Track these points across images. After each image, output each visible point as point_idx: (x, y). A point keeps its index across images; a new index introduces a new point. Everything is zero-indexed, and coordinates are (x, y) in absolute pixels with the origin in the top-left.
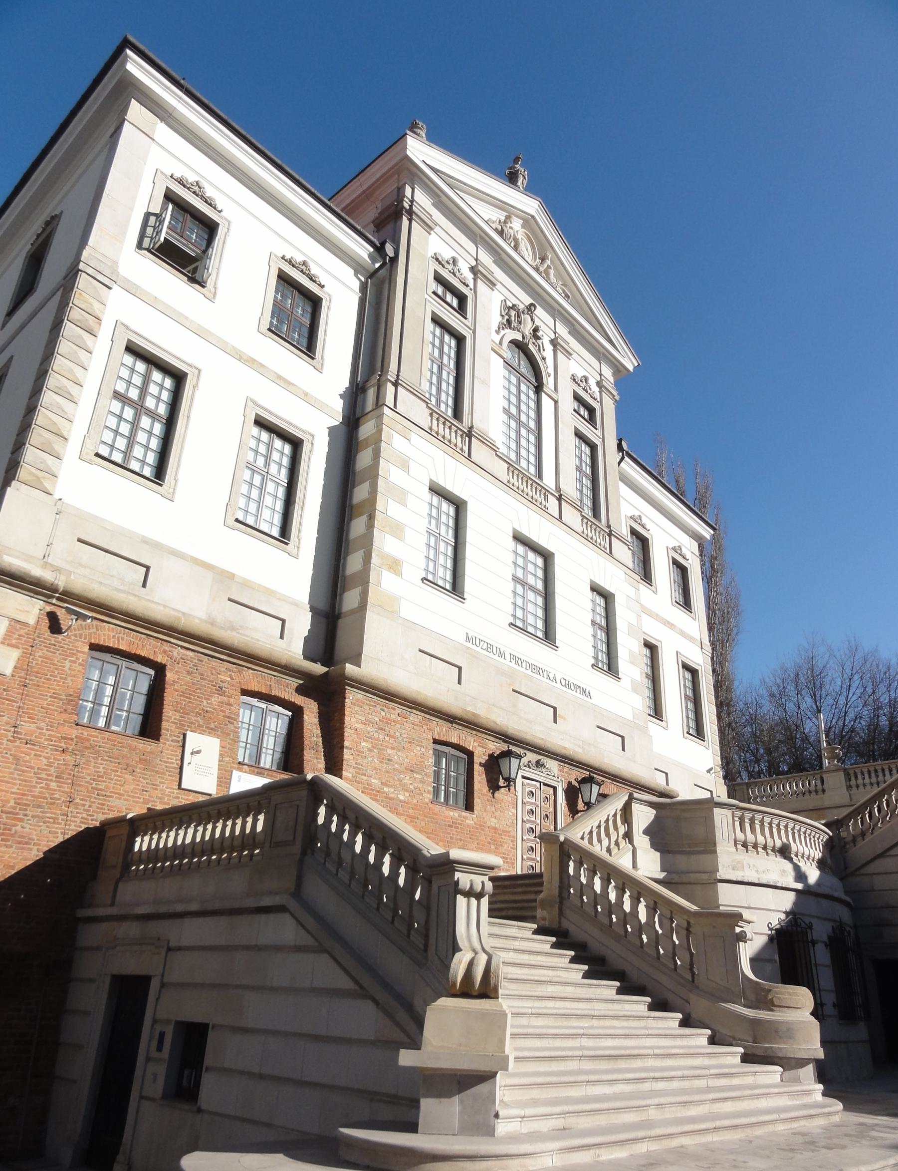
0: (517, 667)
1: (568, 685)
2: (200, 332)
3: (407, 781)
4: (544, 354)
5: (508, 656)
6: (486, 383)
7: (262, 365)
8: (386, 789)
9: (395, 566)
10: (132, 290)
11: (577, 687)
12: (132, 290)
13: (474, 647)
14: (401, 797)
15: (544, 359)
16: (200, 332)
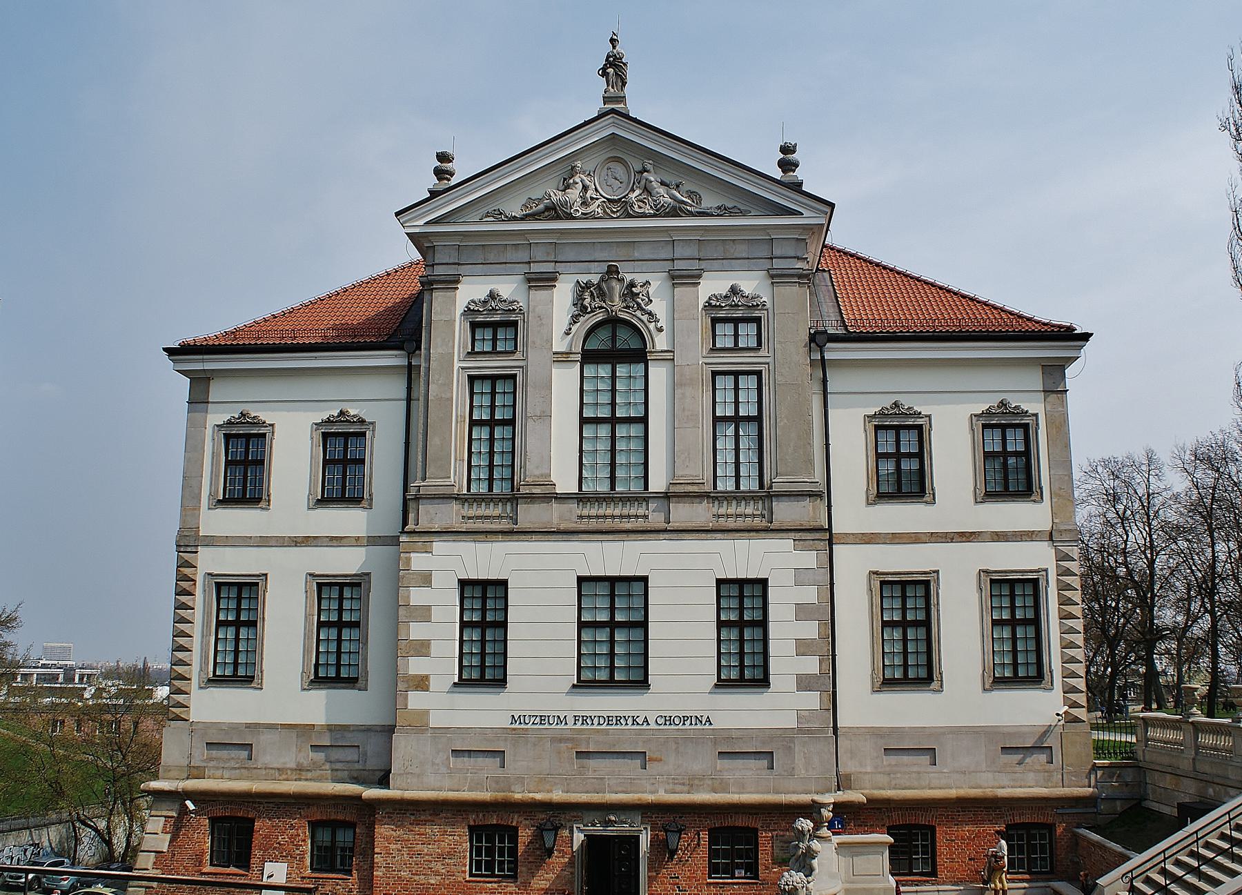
0: (585, 727)
1: (669, 720)
2: (264, 542)
3: (438, 866)
4: (649, 308)
5: (571, 721)
6: (546, 416)
8: (416, 878)
9: (422, 683)
10: (211, 542)
11: (685, 718)
12: (211, 542)
13: (522, 726)
14: (433, 882)
15: (650, 314)
16: (264, 542)
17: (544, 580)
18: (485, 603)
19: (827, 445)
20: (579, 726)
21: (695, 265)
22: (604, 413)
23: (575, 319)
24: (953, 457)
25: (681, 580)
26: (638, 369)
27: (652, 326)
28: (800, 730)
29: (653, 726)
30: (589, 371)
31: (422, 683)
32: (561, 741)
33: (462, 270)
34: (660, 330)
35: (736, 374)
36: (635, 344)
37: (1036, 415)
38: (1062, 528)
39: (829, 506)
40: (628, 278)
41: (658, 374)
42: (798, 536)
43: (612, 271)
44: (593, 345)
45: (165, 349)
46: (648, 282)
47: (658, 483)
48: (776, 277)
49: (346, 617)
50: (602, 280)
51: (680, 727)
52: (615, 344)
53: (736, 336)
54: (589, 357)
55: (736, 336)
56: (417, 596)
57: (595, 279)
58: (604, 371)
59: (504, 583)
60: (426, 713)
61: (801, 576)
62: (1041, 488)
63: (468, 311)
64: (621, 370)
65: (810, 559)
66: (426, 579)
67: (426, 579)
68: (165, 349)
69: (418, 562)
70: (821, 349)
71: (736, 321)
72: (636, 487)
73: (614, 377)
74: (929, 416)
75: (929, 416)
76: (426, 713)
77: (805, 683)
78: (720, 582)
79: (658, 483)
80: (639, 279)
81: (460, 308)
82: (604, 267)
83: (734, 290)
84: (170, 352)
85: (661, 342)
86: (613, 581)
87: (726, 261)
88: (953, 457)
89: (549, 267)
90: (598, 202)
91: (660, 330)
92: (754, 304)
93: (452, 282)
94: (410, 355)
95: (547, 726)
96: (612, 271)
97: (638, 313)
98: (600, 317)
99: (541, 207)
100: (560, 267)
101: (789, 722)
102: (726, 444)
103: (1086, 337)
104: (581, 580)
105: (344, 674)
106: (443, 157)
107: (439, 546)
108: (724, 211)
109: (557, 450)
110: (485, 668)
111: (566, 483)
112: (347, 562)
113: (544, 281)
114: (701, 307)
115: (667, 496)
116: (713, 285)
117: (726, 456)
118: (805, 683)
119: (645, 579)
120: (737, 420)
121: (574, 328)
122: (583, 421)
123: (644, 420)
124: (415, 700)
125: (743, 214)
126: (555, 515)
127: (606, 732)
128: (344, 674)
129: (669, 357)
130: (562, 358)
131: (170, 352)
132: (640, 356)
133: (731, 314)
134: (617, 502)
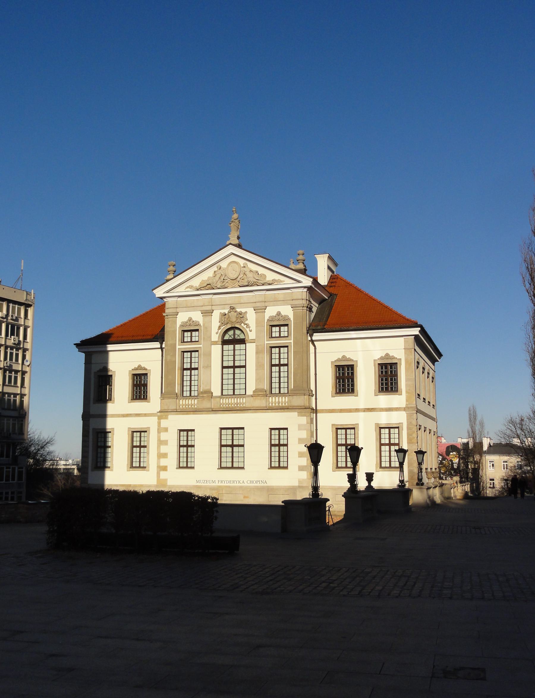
1: (252, 482)
5: (217, 482)
6: (208, 366)
7: (130, 414)
9: (165, 468)
11: (257, 482)
17: (207, 429)
19: (316, 374)
20: (220, 484)
21: (263, 304)
22: (231, 364)
23: (219, 328)
24: (366, 378)
25: (256, 428)
26: (243, 346)
27: (248, 329)
28: (300, 487)
29: (246, 484)
30: (226, 347)
31: (165, 468)
32: (213, 490)
33: (178, 310)
34: (251, 331)
35: (279, 347)
36: (242, 337)
37: (400, 359)
38: (409, 406)
39: (316, 399)
40: (238, 310)
41: (251, 348)
42: (300, 410)
43: (232, 308)
44: (227, 337)
45: (74, 344)
46: (246, 312)
47: (250, 392)
49: (142, 444)
50: (229, 312)
51: (256, 485)
52: (233, 338)
53: (280, 332)
54: (225, 342)
55: (280, 332)
56: (164, 436)
57: (226, 311)
58: (231, 347)
59: (193, 430)
60: (166, 480)
61: (300, 427)
62: (401, 389)
63: (181, 326)
64: (237, 347)
65: (304, 420)
66: (166, 430)
67: (166, 430)
68: (74, 344)
69: (164, 423)
70: (311, 336)
71: (280, 326)
72: (243, 392)
73: (234, 350)
74: (357, 361)
75: (357, 361)
76: (166, 480)
77: (301, 468)
78: (271, 429)
79: (250, 392)
80: (243, 310)
81: (178, 326)
82: (228, 307)
83: (279, 314)
84: (77, 345)
85: (252, 335)
86: (233, 429)
87: (276, 302)
88: (366, 378)
89: (209, 308)
90: (227, 281)
91: (251, 331)
92: (287, 318)
94: (161, 344)
95: (208, 484)
96: (232, 308)
97: (243, 324)
98: (229, 326)
99: (205, 285)
100: (214, 308)
101: (296, 484)
102: (275, 375)
104: (222, 429)
105: (142, 465)
109: (213, 379)
111: (217, 392)
112: (138, 423)
113: (207, 313)
114: (266, 321)
116: (271, 312)
117: (275, 380)
118: (301, 468)
119: (243, 428)
120: (280, 365)
121: (220, 330)
122: (223, 367)
126: (214, 404)
127: (229, 487)
128: (142, 465)
129: (253, 341)
130: (215, 343)
131: (77, 345)
132: (242, 341)
133: (278, 324)
134: (233, 400)
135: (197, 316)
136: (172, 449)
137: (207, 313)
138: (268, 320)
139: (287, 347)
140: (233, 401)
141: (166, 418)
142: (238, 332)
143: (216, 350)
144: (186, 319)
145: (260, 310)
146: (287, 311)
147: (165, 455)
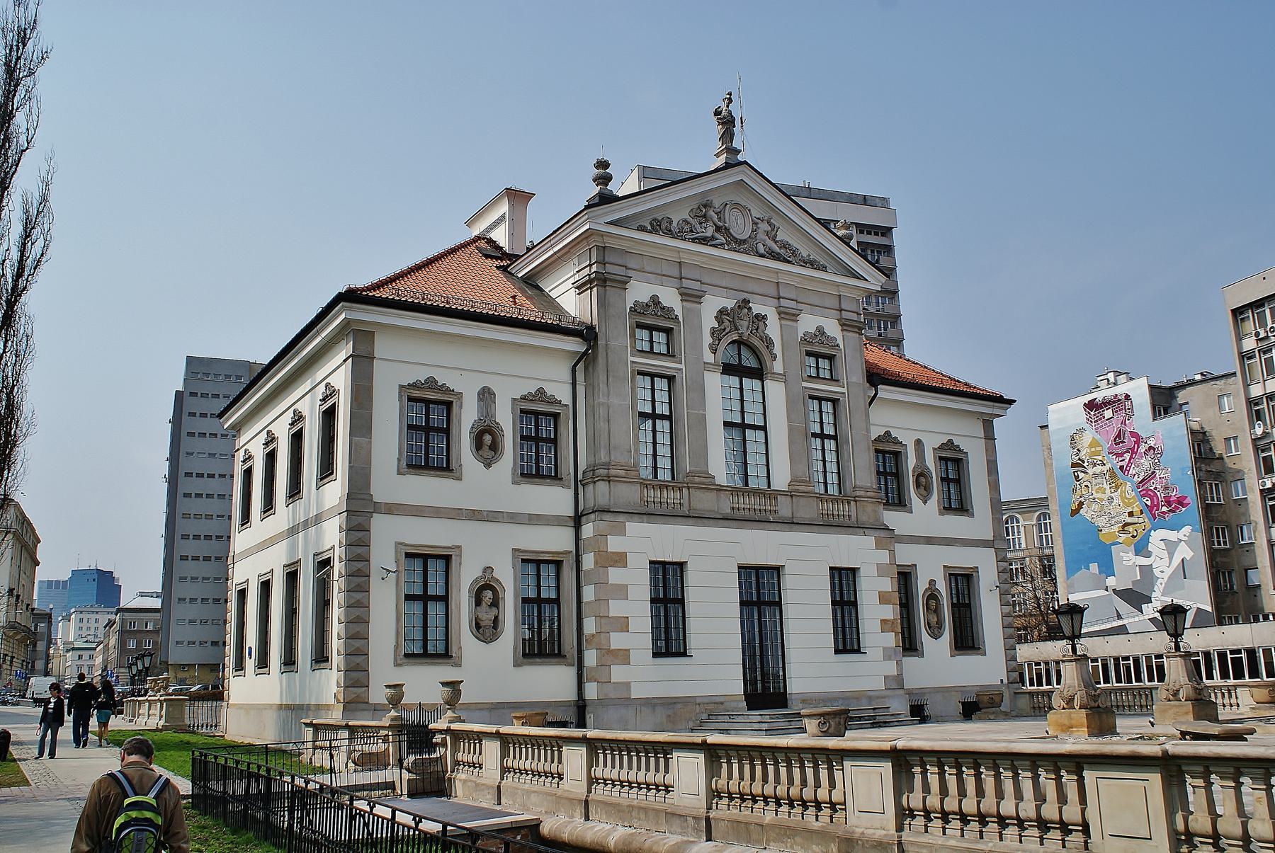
9: (623, 657)
18: (668, 584)
26: (756, 384)
31: (623, 657)
41: (775, 390)
43: (746, 302)
48: (845, 325)
56: (615, 575)
58: (735, 381)
66: (620, 559)
67: (620, 559)
85: (778, 366)
93: (623, 283)
98: (736, 337)
103: (1011, 402)
106: (603, 164)
107: (633, 527)
108: (812, 264)
110: (670, 641)
111: (722, 478)
113: (691, 297)
115: (790, 494)
116: (808, 323)
123: (764, 428)
124: (618, 673)
125: (824, 269)
129: (784, 378)
132: (758, 374)
135: (670, 298)
136: (636, 607)
137: (691, 297)
138: (804, 340)
139: (835, 402)
140: (757, 503)
141: (622, 532)
142: (744, 352)
143: (715, 383)
144: (645, 299)
145: (788, 316)
146: (833, 329)
147: (623, 624)
